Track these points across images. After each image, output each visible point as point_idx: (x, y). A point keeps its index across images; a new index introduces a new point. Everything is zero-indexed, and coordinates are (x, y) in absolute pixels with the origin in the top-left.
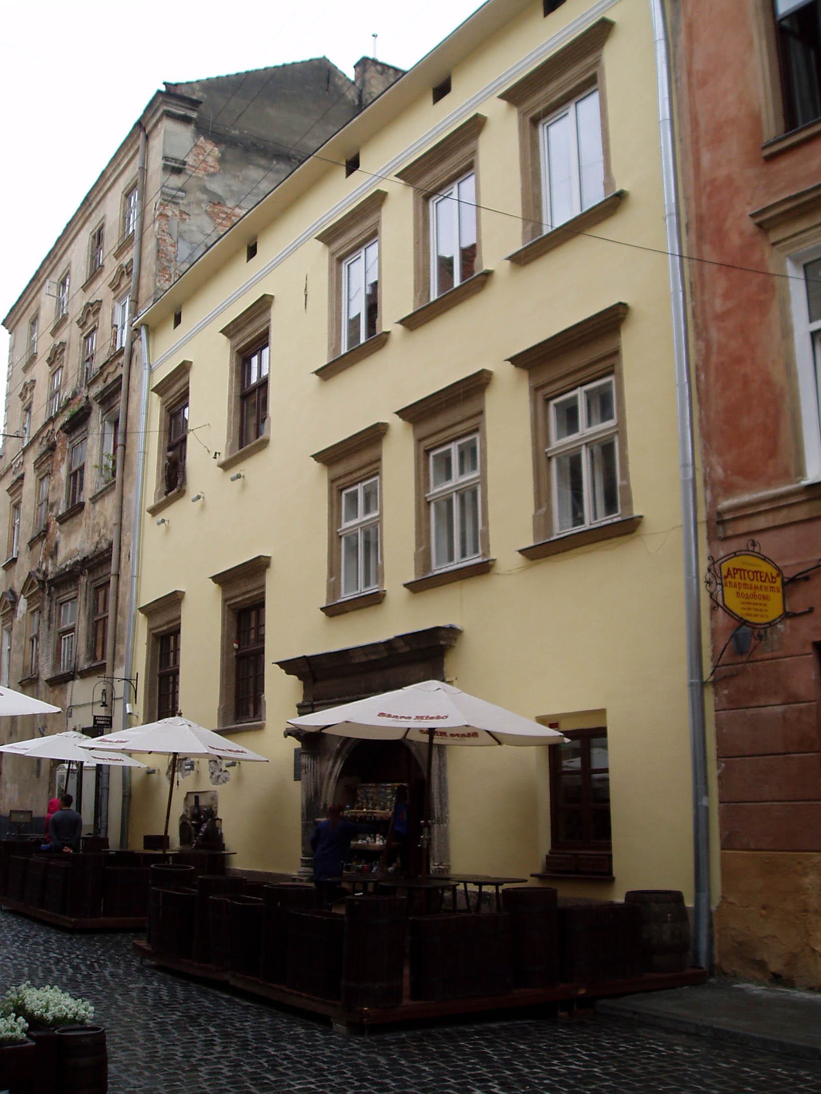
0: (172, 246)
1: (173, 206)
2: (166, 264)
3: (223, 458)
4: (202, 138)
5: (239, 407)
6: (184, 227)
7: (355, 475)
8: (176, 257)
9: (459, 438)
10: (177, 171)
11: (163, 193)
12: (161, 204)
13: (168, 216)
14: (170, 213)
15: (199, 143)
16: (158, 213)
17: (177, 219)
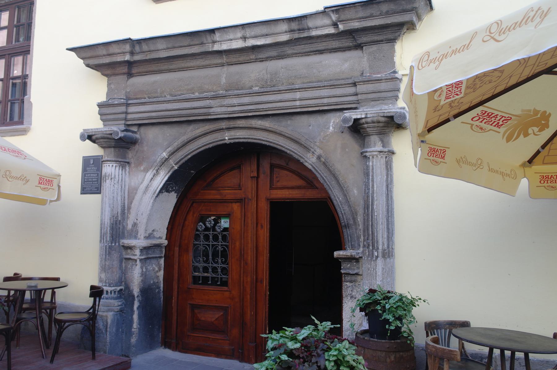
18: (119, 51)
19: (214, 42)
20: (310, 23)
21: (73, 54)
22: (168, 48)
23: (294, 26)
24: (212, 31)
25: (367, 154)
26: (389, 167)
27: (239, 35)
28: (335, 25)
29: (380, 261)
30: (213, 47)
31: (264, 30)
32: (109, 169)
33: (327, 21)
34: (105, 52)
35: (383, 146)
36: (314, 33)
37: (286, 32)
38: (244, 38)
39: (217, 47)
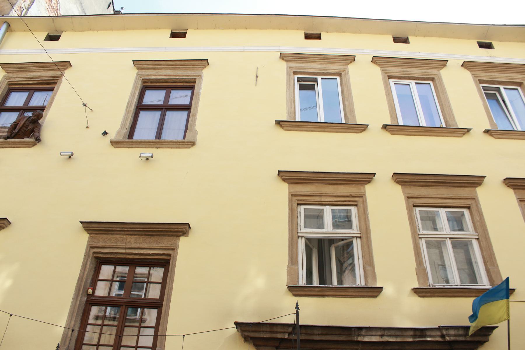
7: (323, 199)
18: (282, 331)
19: (359, 335)
20: (428, 333)
22: (321, 334)
23: (418, 333)
24: (360, 329)
27: (380, 333)
28: (443, 336)
30: (357, 338)
31: (398, 333)
33: (439, 333)
34: (268, 329)
36: (429, 339)
37: (411, 336)
38: (381, 336)
39: (360, 339)
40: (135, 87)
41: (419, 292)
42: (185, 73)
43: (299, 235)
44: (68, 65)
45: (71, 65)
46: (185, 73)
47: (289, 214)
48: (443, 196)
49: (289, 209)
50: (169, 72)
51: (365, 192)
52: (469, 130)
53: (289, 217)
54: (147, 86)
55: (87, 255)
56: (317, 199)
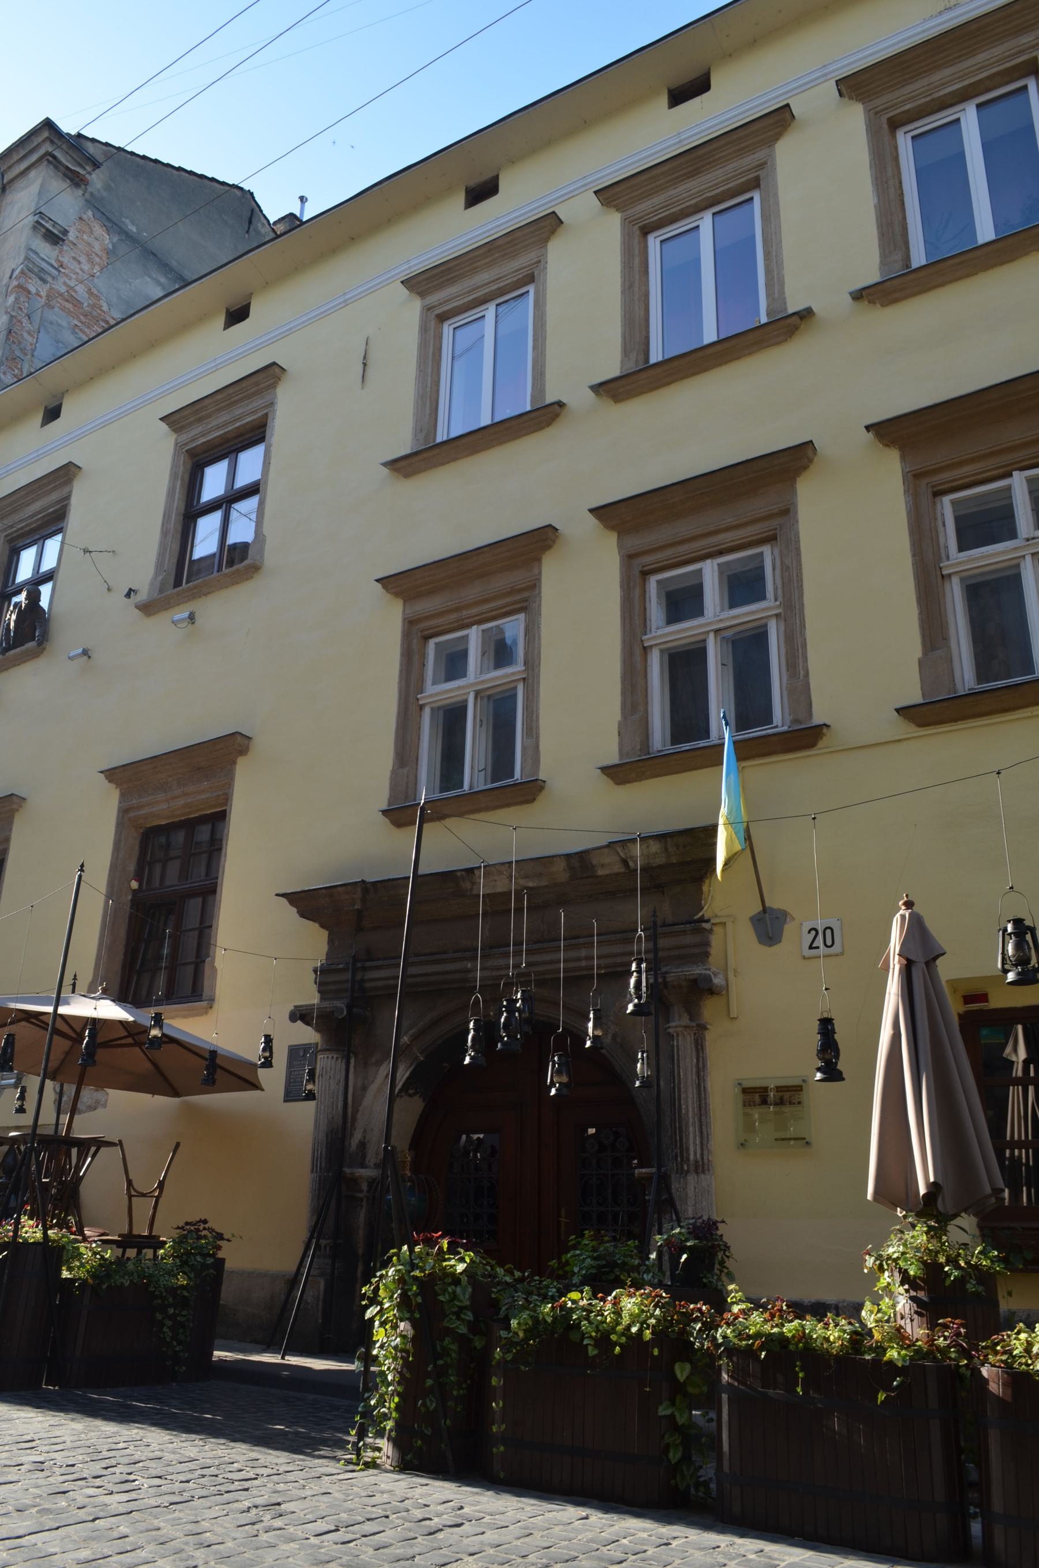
0: (29, 333)
1: (39, 282)
2: (18, 353)
3: (143, 596)
4: (90, 213)
5: (180, 528)
6: (51, 316)
8: (33, 350)
9: (721, 553)
10: (55, 238)
11: (27, 258)
12: (22, 272)
13: (29, 292)
14: (33, 290)
15: (85, 217)
16: (15, 283)
17: (43, 301)
21: (284, 900)
25: (671, 1030)
26: (699, 1047)
29: (691, 1178)
32: (325, 1062)
35: (691, 1020)
40: (174, 476)
41: (618, 773)
42: (250, 407)
43: (421, 702)
44: (73, 469)
45: (79, 468)
46: (250, 407)
47: (401, 665)
48: (711, 528)
49: (402, 655)
50: (224, 417)
51: (540, 573)
52: (806, 315)
53: (401, 671)
54: (196, 463)
55: (120, 825)
56: (454, 616)
